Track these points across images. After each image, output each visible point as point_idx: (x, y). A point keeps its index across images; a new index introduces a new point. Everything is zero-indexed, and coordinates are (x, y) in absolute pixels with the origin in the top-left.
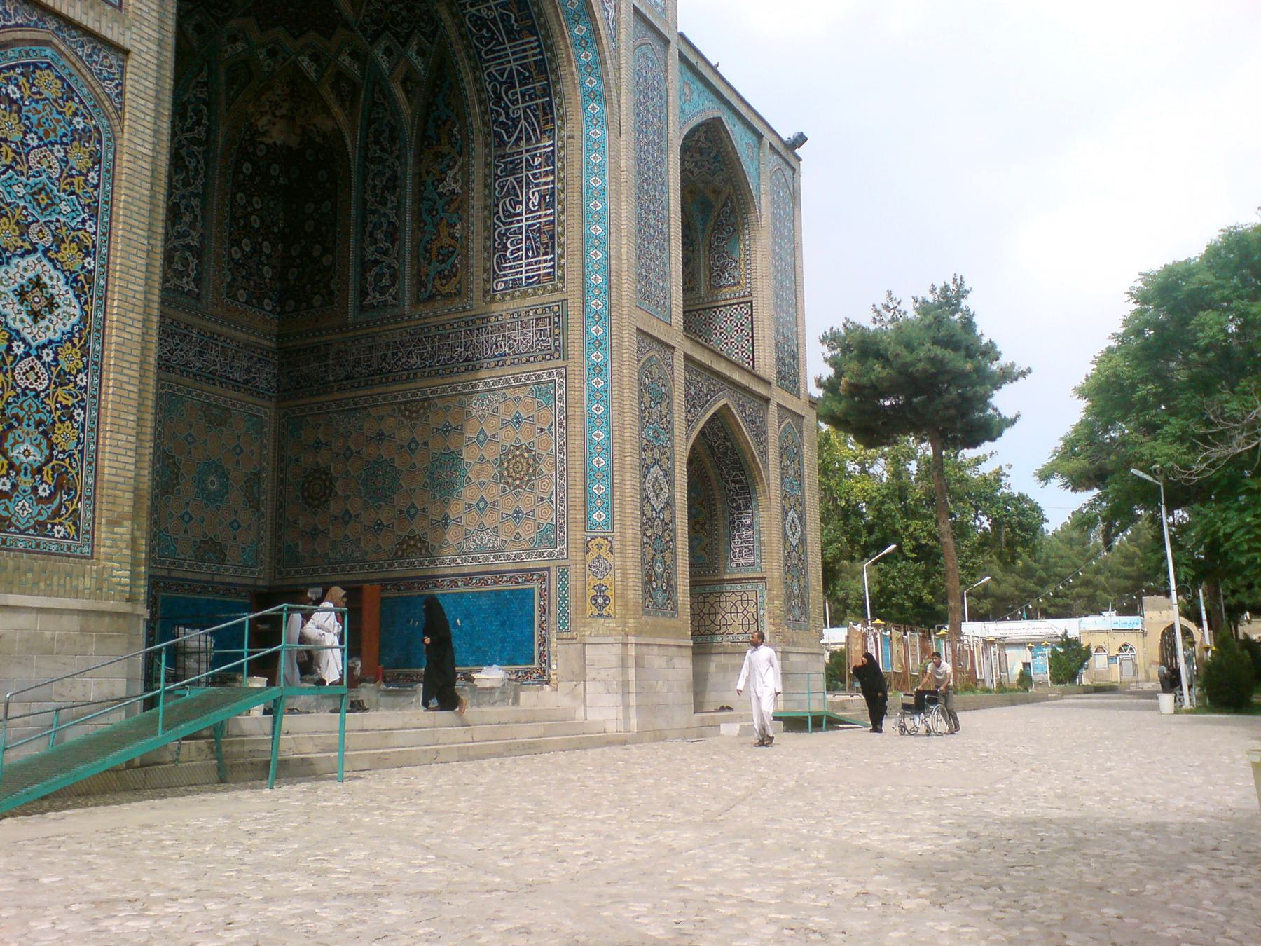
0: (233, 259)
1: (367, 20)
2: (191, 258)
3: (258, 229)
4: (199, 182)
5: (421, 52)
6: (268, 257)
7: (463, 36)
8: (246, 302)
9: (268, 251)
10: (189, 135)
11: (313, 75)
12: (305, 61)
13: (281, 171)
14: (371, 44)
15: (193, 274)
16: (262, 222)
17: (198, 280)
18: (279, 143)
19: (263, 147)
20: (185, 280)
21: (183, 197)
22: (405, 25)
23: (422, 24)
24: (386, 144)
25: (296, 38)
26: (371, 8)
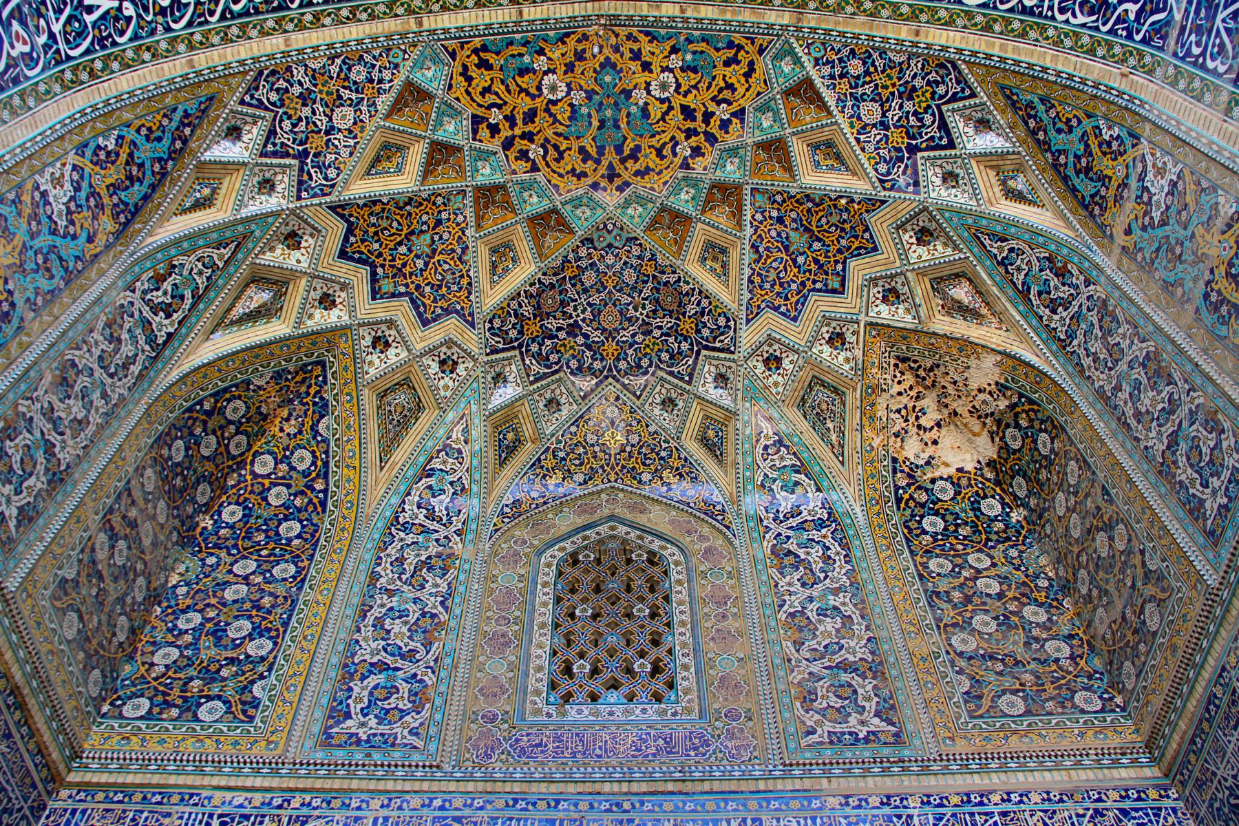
0: (961, 654)
1: (883, 168)
2: (857, 681)
3: (1000, 596)
4: (839, 572)
5: (983, 125)
6: (1043, 627)
7: (988, 28)
8: (1028, 712)
9: (1042, 617)
10: (793, 522)
11: (909, 318)
12: (884, 313)
13: (1003, 504)
14: (917, 193)
15: (871, 706)
16: (1003, 579)
17: (886, 711)
18: (969, 467)
19: (939, 483)
20: (853, 720)
21: (811, 599)
22: (928, 119)
23: (941, 90)
24: (1064, 292)
25: (841, 291)
26: (870, 148)
